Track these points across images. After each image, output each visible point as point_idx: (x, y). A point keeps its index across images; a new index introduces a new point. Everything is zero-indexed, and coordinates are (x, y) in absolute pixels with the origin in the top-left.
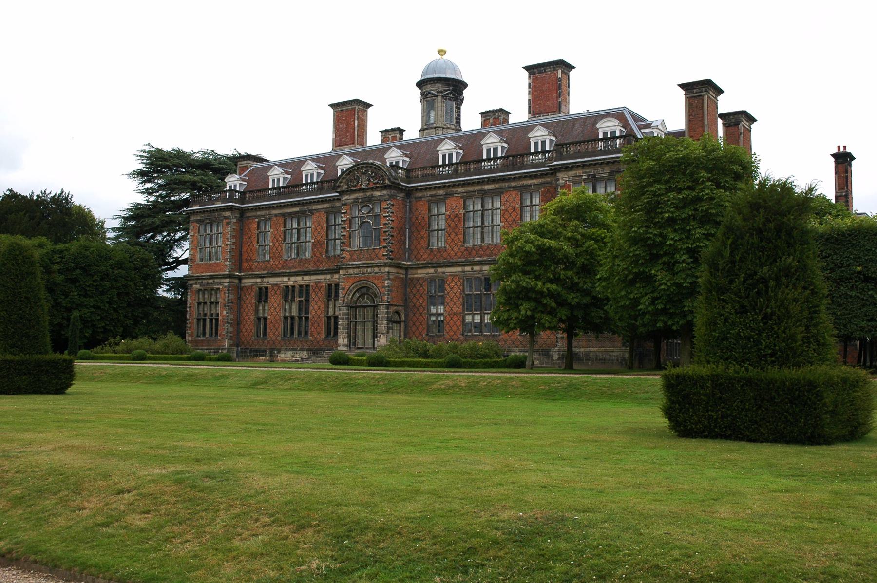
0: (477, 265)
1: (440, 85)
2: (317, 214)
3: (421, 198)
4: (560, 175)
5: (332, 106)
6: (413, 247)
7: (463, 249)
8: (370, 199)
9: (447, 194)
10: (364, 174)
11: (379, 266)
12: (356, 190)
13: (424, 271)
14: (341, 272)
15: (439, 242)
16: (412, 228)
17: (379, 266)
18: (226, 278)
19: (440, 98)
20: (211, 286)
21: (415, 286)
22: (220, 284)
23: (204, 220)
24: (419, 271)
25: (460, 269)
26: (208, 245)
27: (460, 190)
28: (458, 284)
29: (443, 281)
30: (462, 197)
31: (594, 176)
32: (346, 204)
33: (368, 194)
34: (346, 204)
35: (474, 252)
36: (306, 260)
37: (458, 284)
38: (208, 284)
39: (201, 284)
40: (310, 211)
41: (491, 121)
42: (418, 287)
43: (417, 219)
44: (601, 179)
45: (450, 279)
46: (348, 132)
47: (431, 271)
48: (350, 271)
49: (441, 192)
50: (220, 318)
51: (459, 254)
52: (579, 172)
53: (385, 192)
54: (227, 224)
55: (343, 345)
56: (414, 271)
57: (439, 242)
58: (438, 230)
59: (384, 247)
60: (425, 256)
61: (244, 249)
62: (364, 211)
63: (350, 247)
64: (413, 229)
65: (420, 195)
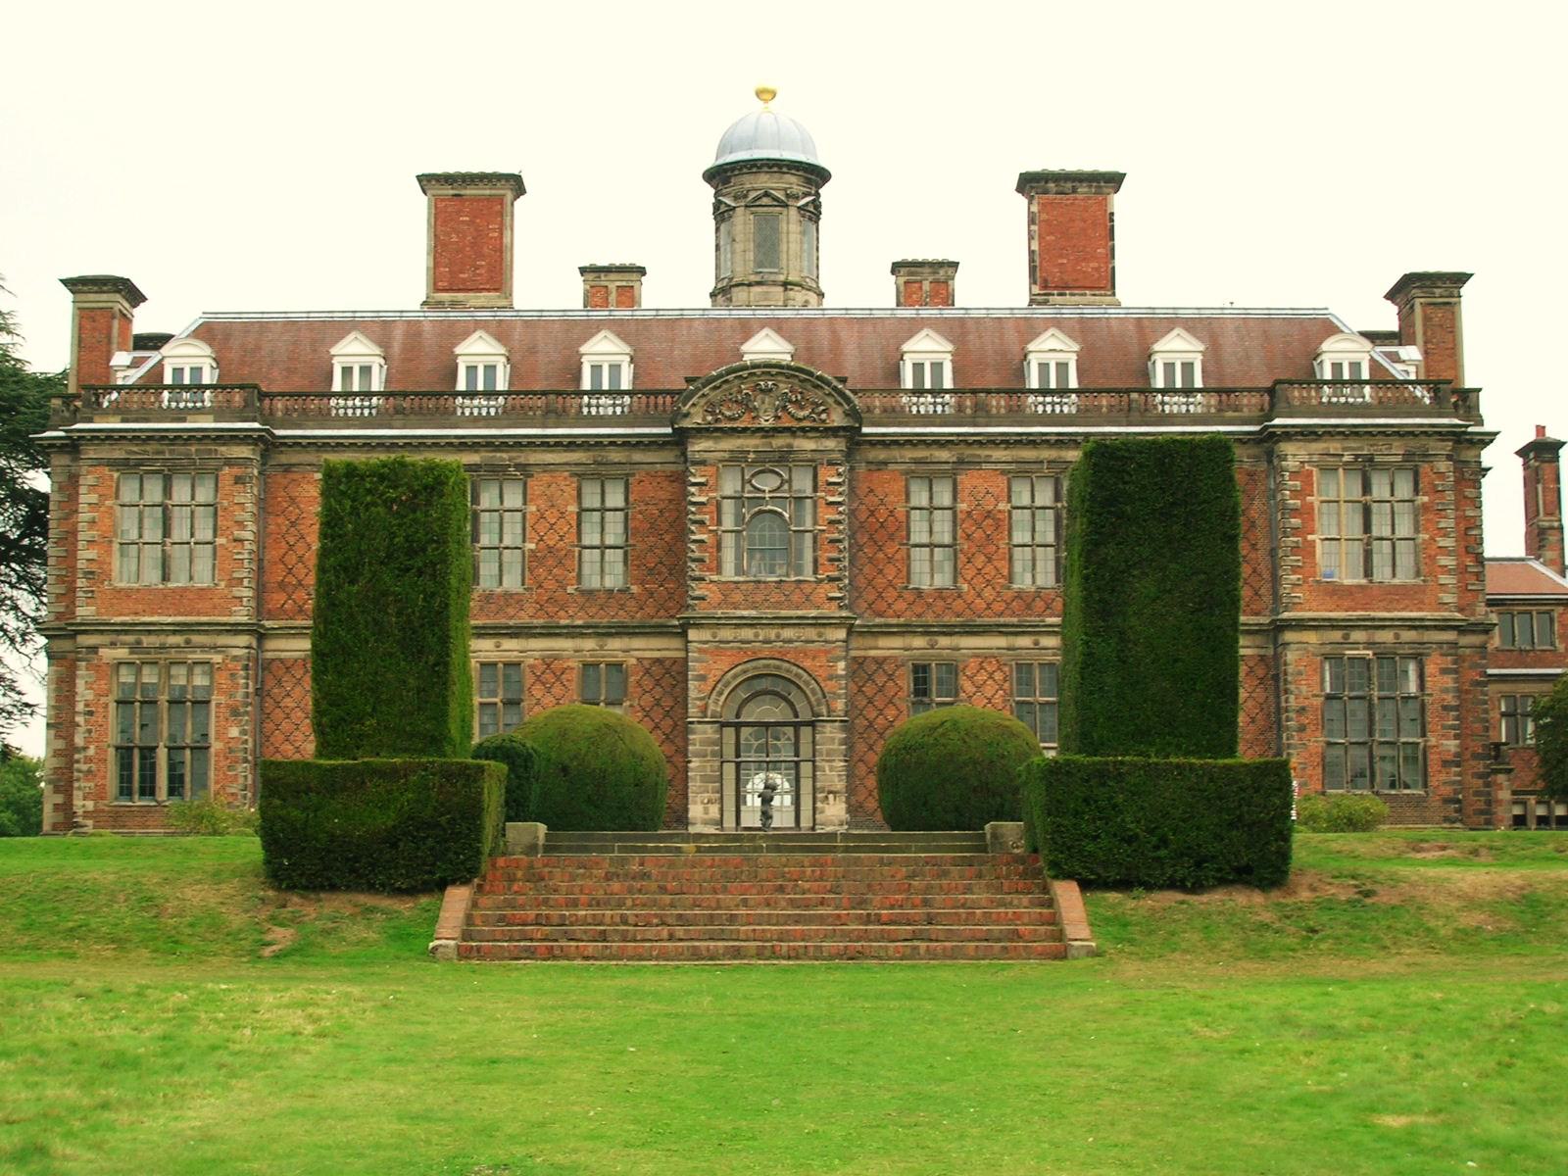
0: (1048, 633)
1: (793, 179)
2: (546, 477)
3: (886, 463)
4: (1288, 448)
5: (426, 181)
6: (861, 582)
7: (1010, 594)
8: (785, 458)
9: (961, 462)
10: (767, 391)
11: (819, 623)
12: (745, 430)
13: (897, 642)
14: (692, 634)
15: (929, 573)
16: (874, 537)
17: (819, 623)
18: (237, 632)
19: (793, 212)
20: (173, 654)
21: (870, 678)
22: (214, 648)
23: (140, 463)
24: (883, 642)
25: (1001, 642)
26: (153, 533)
27: (999, 454)
28: (998, 676)
29: (952, 669)
30: (1003, 472)
31: (1370, 459)
32: (703, 463)
33: (779, 442)
34: (703, 463)
35: (1039, 604)
36: (508, 596)
37: (998, 676)
38: (163, 647)
39: (135, 648)
40: (517, 466)
41: (926, 286)
42: (881, 680)
43: (872, 513)
44: (1384, 467)
45: (973, 664)
46: (481, 256)
47: (919, 642)
48: (726, 634)
49: (944, 455)
50: (216, 746)
51: (998, 607)
52: (1334, 446)
53: (830, 444)
54: (238, 480)
55: (706, 823)
56: (869, 641)
57: (929, 573)
58: (931, 546)
59: (831, 579)
60: (900, 606)
61: (272, 555)
62: (767, 484)
63: (719, 570)
64: (863, 539)
65: (881, 454)
